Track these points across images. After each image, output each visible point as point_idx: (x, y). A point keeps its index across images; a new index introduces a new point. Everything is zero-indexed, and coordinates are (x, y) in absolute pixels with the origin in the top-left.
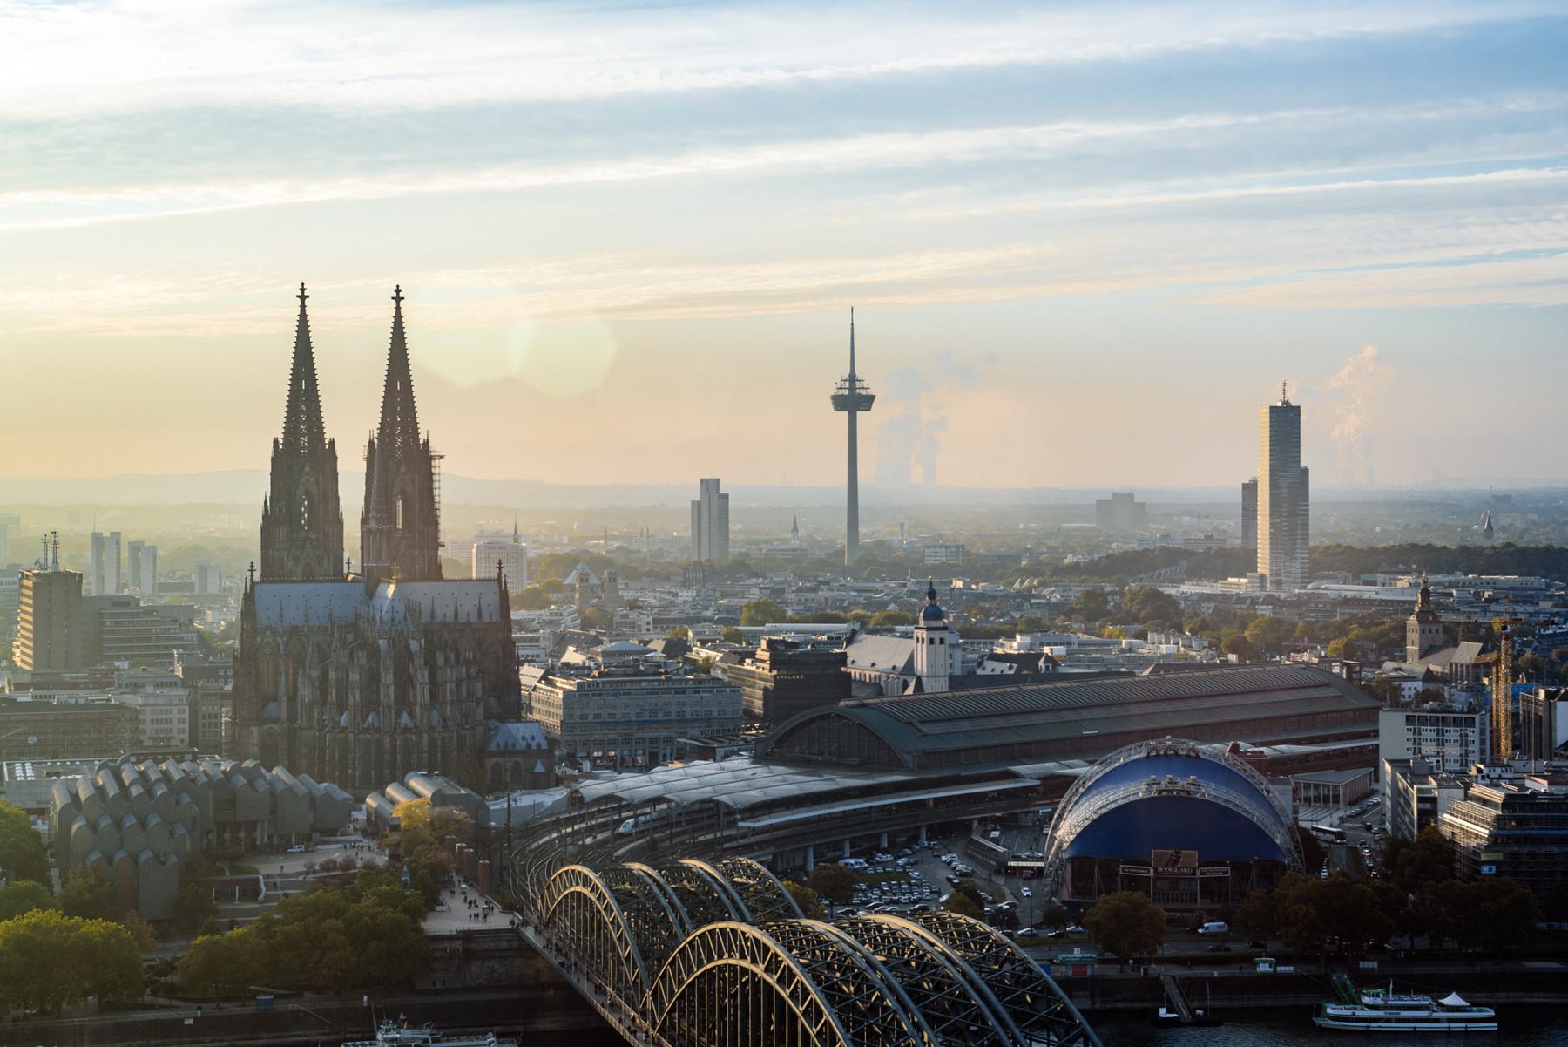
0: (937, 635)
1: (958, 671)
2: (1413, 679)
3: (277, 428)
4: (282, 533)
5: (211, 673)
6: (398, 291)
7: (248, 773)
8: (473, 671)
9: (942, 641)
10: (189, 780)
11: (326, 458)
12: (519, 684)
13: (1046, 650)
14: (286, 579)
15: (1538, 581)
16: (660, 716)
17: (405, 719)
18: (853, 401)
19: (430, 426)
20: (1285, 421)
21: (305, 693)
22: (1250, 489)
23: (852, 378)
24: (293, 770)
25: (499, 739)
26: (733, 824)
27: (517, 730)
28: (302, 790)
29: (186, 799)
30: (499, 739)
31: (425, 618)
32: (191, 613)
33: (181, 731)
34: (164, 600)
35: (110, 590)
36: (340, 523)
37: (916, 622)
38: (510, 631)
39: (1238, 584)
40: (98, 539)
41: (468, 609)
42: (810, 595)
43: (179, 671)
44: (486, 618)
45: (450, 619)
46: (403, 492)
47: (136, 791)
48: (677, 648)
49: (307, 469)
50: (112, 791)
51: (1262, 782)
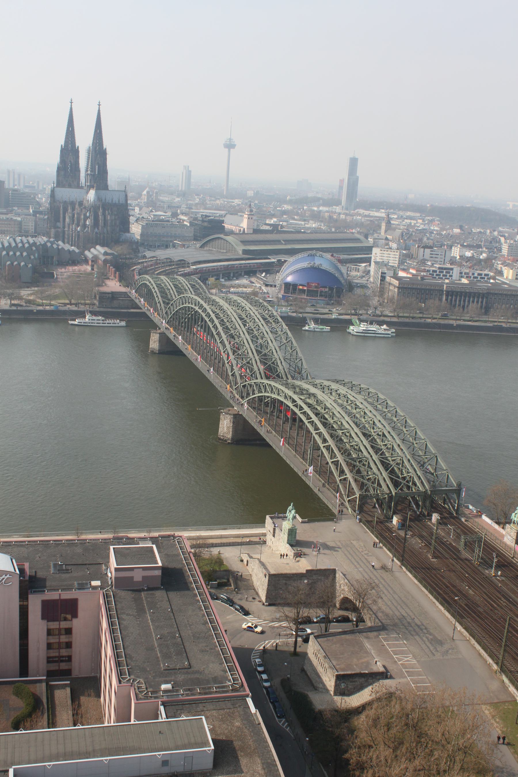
0: (251, 217)
1: (255, 228)
2: (382, 239)
3: (62, 142)
4: (62, 173)
5: (41, 213)
6: (99, 103)
7: (51, 242)
8: (116, 217)
9: (252, 218)
10: (34, 244)
11: (76, 152)
12: (129, 222)
13: (281, 223)
14: (64, 186)
15: (418, 215)
16: (169, 234)
17: (96, 230)
18: (230, 146)
19: (106, 144)
20: (354, 163)
21: (67, 220)
22: (342, 181)
23: (230, 139)
24: (64, 242)
25: (123, 237)
26: (189, 267)
27: (127, 234)
28: (66, 249)
29: (34, 248)
30: (123, 237)
31: (103, 201)
32: (36, 194)
33: (32, 229)
34: (27, 190)
35: (11, 186)
36: (79, 171)
37: (244, 212)
38: (127, 206)
39: (338, 209)
40: (9, 172)
41: (116, 200)
42: (214, 202)
43: (31, 211)
44: (121, 202)
45: (110, 202)
46: (98, 163)
47: (20, 245)
48: (175, 215)
49: (71, 154)
50: (13, 245)
51: (339, 265)
